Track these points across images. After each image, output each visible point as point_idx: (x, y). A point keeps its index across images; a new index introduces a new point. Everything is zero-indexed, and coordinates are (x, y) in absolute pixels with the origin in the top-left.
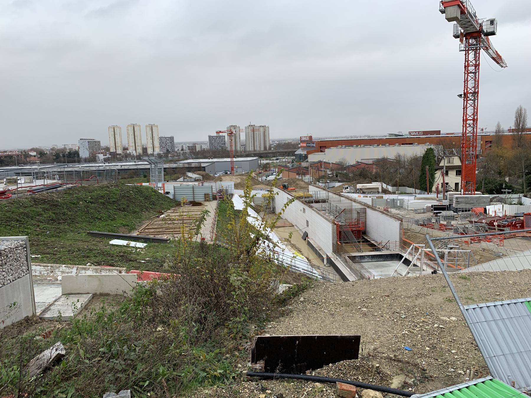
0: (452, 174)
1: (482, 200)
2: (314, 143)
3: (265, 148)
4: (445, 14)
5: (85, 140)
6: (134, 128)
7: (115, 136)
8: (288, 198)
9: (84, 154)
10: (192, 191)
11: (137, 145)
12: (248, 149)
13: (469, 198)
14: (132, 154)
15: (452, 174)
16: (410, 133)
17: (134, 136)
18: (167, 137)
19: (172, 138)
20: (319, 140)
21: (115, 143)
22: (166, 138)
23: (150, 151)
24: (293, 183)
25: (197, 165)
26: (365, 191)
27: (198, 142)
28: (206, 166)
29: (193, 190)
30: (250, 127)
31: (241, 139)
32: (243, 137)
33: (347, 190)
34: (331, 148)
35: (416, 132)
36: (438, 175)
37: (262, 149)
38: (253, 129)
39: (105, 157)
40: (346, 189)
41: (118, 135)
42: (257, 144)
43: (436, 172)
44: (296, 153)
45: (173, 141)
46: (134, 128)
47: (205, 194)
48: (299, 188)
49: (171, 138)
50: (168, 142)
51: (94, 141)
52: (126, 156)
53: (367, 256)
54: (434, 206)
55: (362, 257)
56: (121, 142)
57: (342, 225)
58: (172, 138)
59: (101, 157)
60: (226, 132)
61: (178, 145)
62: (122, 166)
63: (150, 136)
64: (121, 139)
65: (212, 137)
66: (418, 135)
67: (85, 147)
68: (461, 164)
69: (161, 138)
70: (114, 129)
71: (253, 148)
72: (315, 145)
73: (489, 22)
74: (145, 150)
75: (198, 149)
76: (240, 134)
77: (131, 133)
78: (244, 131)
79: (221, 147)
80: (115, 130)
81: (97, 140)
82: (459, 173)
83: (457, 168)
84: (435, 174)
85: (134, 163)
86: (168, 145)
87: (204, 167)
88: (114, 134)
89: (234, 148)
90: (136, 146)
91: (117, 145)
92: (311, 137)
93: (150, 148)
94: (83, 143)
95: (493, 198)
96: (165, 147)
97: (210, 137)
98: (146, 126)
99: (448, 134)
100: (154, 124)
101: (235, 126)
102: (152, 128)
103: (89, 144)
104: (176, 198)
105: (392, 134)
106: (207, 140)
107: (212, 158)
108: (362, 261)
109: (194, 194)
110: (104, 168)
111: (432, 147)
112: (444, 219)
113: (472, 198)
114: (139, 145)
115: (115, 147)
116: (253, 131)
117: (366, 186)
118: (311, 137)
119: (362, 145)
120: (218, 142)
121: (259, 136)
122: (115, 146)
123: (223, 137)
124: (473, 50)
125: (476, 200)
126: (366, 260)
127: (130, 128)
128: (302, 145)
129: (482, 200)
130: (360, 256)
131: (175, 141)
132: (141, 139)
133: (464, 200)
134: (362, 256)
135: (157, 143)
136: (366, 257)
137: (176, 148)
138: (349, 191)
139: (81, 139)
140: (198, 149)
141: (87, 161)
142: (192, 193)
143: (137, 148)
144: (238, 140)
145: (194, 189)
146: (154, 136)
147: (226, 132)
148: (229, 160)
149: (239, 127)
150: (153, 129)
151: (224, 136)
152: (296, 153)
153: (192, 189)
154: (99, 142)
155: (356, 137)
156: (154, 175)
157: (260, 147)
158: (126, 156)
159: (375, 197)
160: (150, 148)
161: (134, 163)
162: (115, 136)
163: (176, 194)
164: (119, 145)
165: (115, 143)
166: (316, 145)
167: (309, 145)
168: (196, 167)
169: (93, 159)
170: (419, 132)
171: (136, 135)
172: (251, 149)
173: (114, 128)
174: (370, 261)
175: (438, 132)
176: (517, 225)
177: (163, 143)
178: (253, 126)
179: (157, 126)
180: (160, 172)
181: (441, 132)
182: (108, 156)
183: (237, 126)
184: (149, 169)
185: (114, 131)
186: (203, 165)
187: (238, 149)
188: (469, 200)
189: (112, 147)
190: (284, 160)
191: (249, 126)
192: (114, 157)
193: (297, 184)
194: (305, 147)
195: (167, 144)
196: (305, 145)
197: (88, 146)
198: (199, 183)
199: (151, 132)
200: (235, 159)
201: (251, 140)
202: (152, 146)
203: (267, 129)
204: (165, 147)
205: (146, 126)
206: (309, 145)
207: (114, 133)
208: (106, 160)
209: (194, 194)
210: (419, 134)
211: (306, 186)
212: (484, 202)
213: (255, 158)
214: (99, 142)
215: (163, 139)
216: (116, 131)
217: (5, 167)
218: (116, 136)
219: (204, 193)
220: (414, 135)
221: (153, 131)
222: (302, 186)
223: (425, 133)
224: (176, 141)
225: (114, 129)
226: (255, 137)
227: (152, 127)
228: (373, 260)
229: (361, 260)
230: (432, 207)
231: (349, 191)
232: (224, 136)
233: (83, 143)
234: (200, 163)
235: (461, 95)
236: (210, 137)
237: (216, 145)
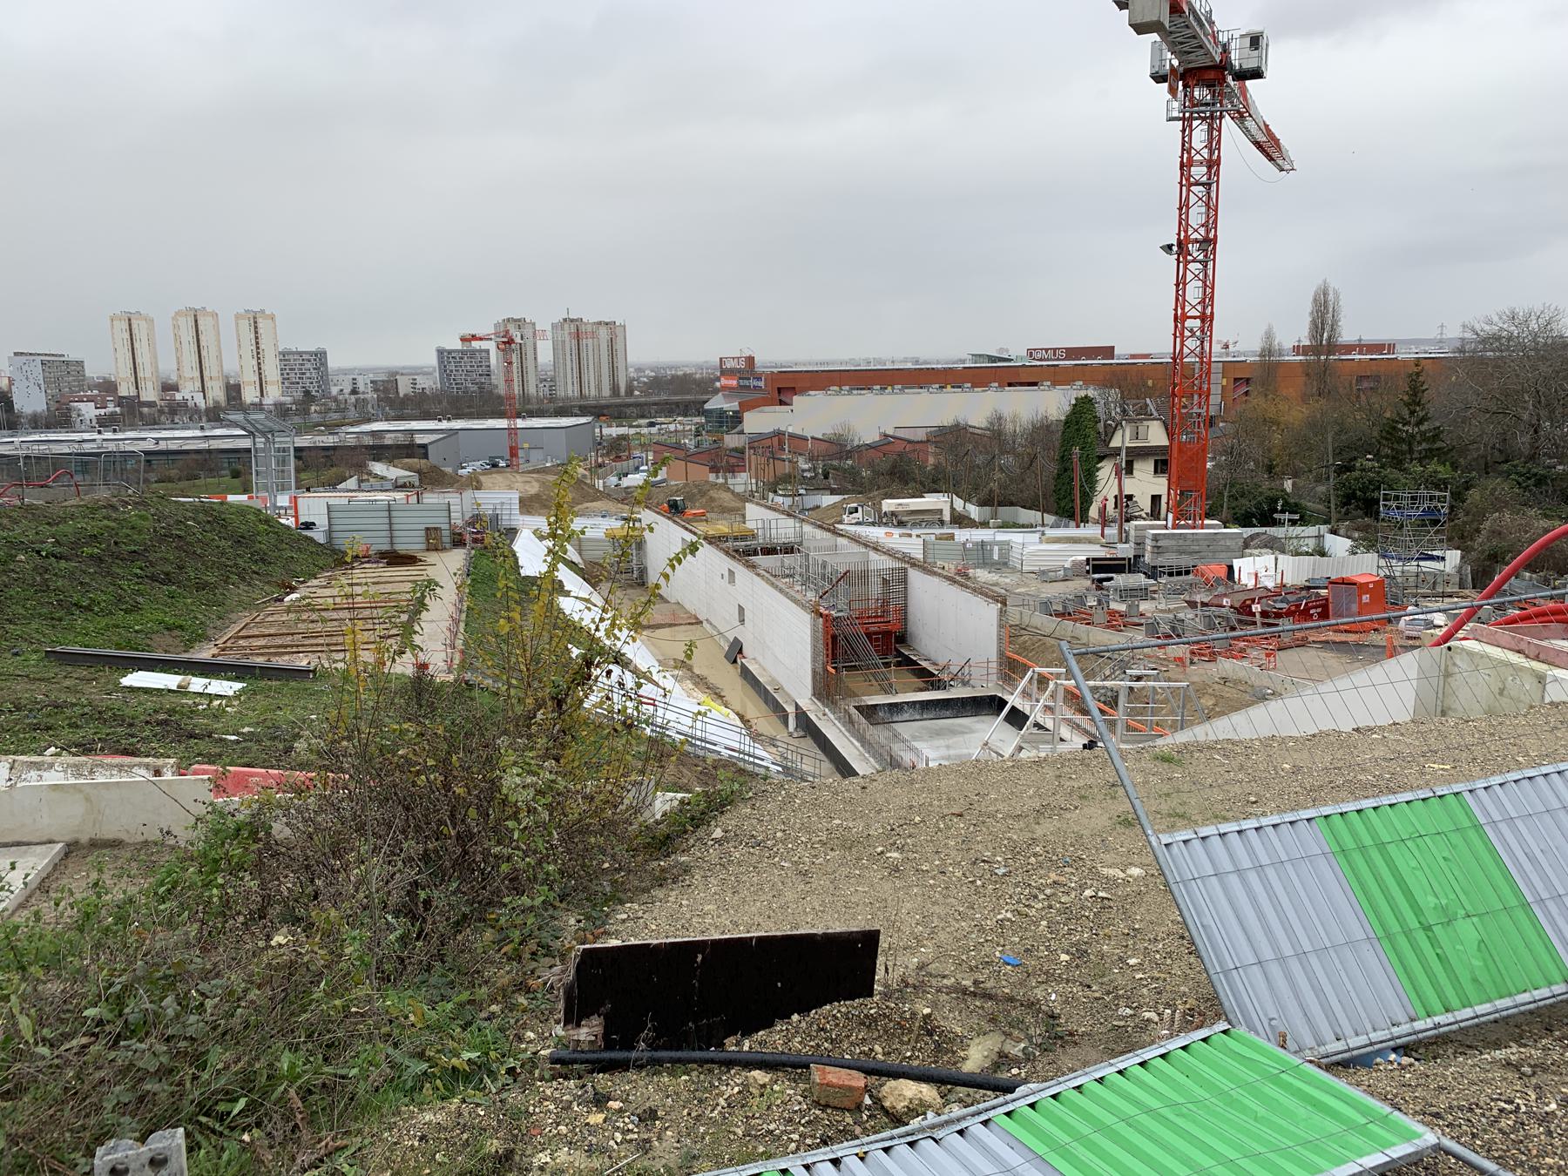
0: (1144, 469)
1: (1222, 543)
2: (759, 379)
3: (615, 389)
4: (1127, 11)
5: (32, 358)
6: (196, 321)
7: (132, 344)
8: (683, 539)
9: (30, 401)
10: (387, 521)
11: (206, 374)
12: (561, 393)
13: (1188, 537)
14: (190, 403)
15: (1144, 469)
16: (1030, 353)
17: (199, 346)
18: (306, 353)
19: (320, 356)
20: (775, 370)
21: (135, 368)
22: (301, 354)
23: (250, 395)
25: (401, 439)
26: (904, 519)
27: (404, 368)
28: (430, 443)
29: (390, 517)
30: (566, 326)
31: (540, 359)
32: (545, 353)
33: (854, 515)
34: (811, 392)
35: (1047, 350)
36: (1106, 471)
37: (606, 392)
38: (576, 331)
39: (102, 412)
40: (851, 513)
41: (145, 342)
42: (590, 377)
43: (1099, 465)
44: (707, 406)
45: (324, 364)
46: (196, 321)
47: (427, 529)
49: (316, 355)
50: (308, 365)
52: (174, 411)
53: (907, 703)
54: (1094, 559)
55: (895, 708)
56: (155, 364)
57: (840, 617)
58: (320, 356)
59: (89, 411)
60: (493, 337)
61: (341, 377)
62: (157, 440)
63: (248, 347)
64: (155, 357)
65: (450, 352)
66: (1051, 360)
67: (31, 380)
68: (1166, 443)
69: (284, 356)
70: (130, 325)
72: (762, 384)
73: (1248, 40)
74: (233, 391)
75: (404, 388)
76: (535, 344)
77: (188, 336)
78: (549, 334)
79: (477, 384)
80: (134, 326)
81: (73, 356)
82: (1161, 467)
83: (1157, 454)
84: (1098, 469)
85: (198, 433)
86: (308, 375)
87: (424, 446)
88: (132, 339)
89: (517, 390)
90: (206, 379)
91: (140, 374)
92: (750, 360)
93: (249, 384)
94: (25, 368)
95: (1252, 537)
96: (298, 383)
97: (441, 352)
98: (238, 317)
99: (1133, 356)
100: (263, 311)
101: (519, 320)
102: (255, 322)
103: (47, 369)
104: (336, 541)
105: (980, 355)
106: (432, 360)
107: (449, 419)
110: (99, 448)
111: (1091, 393)
112: (1121, 597)
113: (1195, 537)
114: (215, 374)
115: (133, 379)
116: (578, 335)
117: (908, 505)
118: (750, 360)
119: (896, 387)
120: (469, 368)
121: (594, 352)
122: (136, 378)
123: (484, 354)
124: (1204, 119)
125: (1207, 543)
126: (906, 716)
127: (182, 321)
128: (724, 381)
129: (1222, 543)
130: (891, 704)
131: (330, 364)
132: (219, 358)
133: (1173, 543)
134: (896, 705)
135: (272, 371)
137: (335, 385)
139: (16, 354)
140: (404, 388)
141: (37, 423)
143: (208, 384)
144: (530, 364)
145: (394, 514)
146: (262, 346)
147: (491, 339)
148: (502, 423)
149: (534, 324)
150: (260, 325)
151: (487, 351)
152: (707, 406)
154: (80, 363)
155: (880, 364)
156: (263, 470)
157: (599, 388)
158: (174, 411)
159: (933, 537)
160: (249, 384)
161: (198, 433)
162: (132, 344)
163: (335, 528)
164: (148, 375)
165: (135, 368)
166: (766, 386)
167: (746, 383)
168: (398, 447)
169: (60, 418)
170: (1055, 350)
171: (202, 344)
172: (570, 393)
173: (130, 320)
174: (918, 717)
175: (1108, 352)
176: (1311, 612)
177: (290, 369)
178: (576, 320)
179: (272, 318)
181: (1116, 352)
182: (111, 408)
183: (528, 320)
184: (248, 451)
185: (131, 330)
186: (420, 439)
187: (532, 390)
188: (1188, 543)
189: (123, 380)
190: (672, 427)
191: (565, 320)
192: (132, 412)
193: (712, 499)
194: (733, 388)
195: (304, 374)
196: (734, 383)
197: (41, 377)
198: (408, 496)
199: (253, 336)
200: (520, 423)
201: (570, 364)
203: (619, 331)
204: (298, 383)
205: (238, 317)
206: (746, 383)
207: (131, 335)
208: (104, 423)
210: (1055, 355)
212: (1228, 549)
213: (583, 420)
214: (80, 363)
215: (291, 357)
216: (135, 331)
218: (136, 345)
219: (423, 527)
220: (1041, 360)
221: (260, 331)
223: (1072, 353)
224: (333, 363)
225: (130, 325)
226: (583, 355)
227: (255, 318)
228: (925, 716)
229: (892, 715)
230: (1088, 564)
232: (487, 351)
233: (25, 368)
234: (412, 432)
235: (1170, 247)
236: (441, 352)
237: (461, 378)
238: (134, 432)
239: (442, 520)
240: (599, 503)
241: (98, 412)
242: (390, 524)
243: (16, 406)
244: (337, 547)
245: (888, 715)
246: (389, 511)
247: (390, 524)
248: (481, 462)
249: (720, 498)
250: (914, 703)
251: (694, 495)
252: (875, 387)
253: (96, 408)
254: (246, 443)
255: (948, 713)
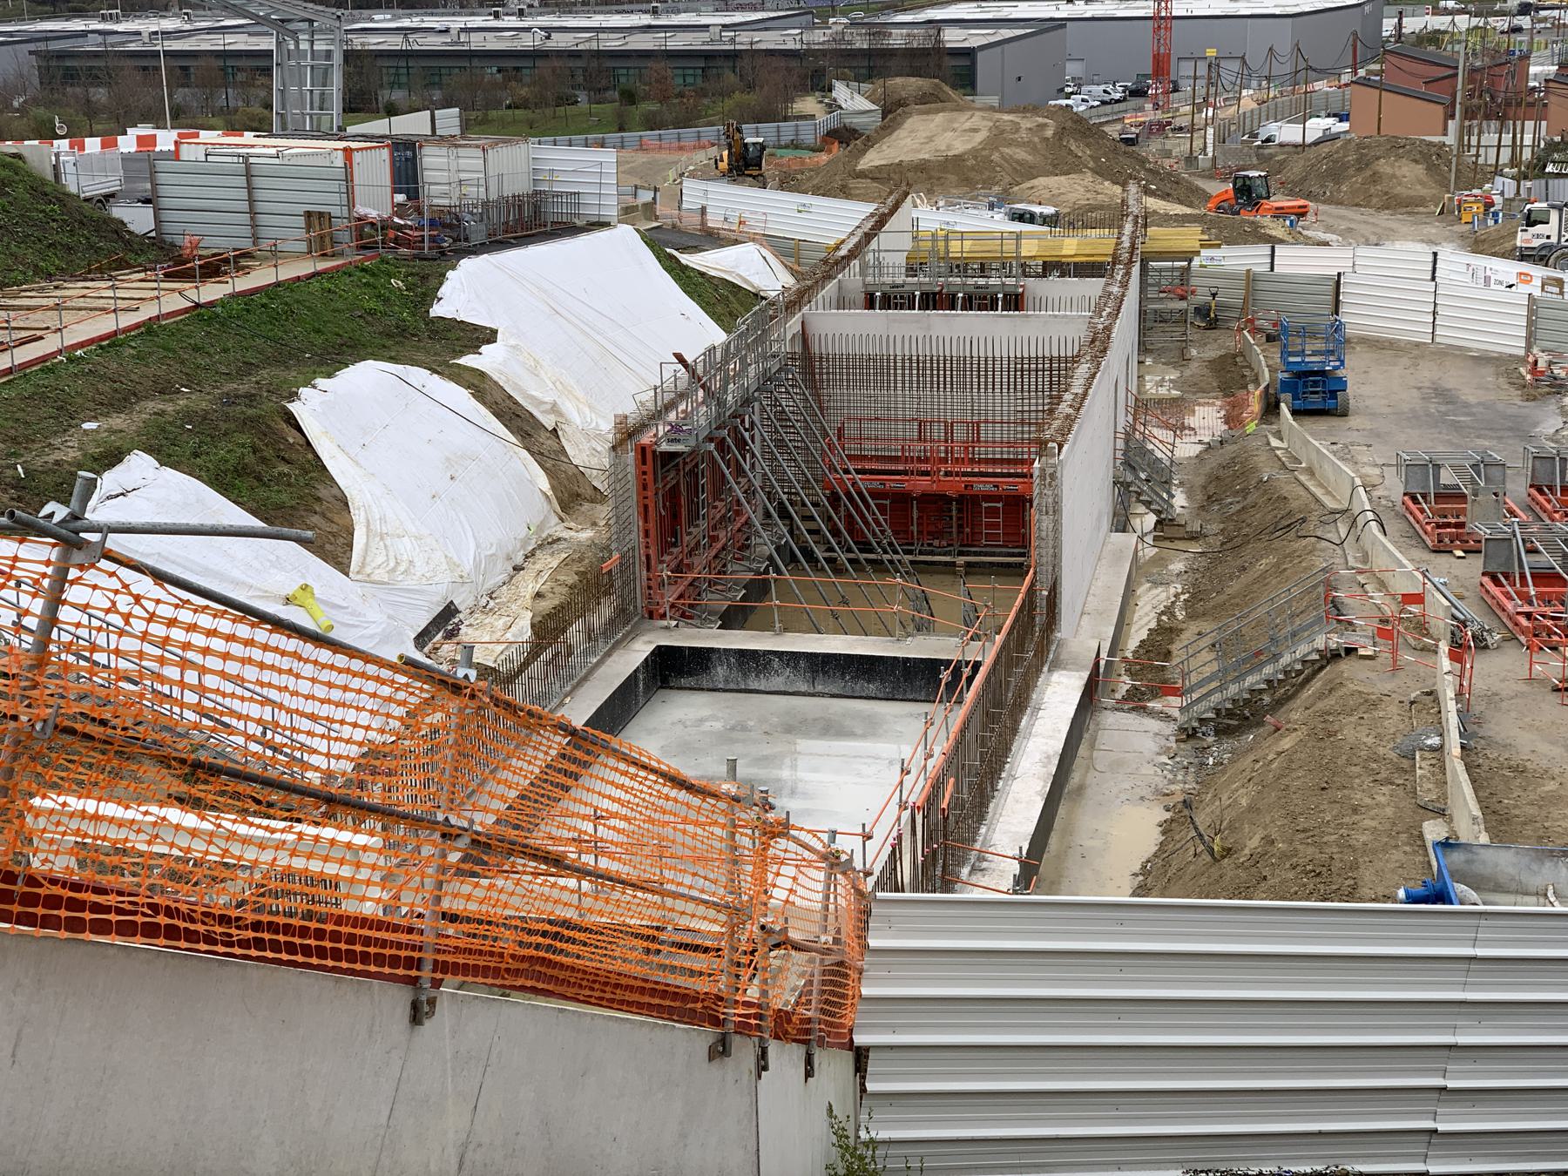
10: (244, 194)
24: (1351, 171)
29: (250, 188)
33: (1539, 228)
47: (308, 214)
48: (1375, 200)
62: (549, 31)
85: (646, 19)
87: (969, 53)
104: (167, 228)
108: (754, 685)
109: (253, 213)
110: (453, 43)
126: (777, 682)
130: (742, 654)
134: (754, 654)
136: (776, 663)
138: (1554, 240)
142: (245, 206)
145: (257, 182)
153: (242, 181)
161: (646, 19)
163: (260, 207)
168: (910, 53)
174: (804, 688)
180: (324, 77)
184: (268, 54)
186: (953, 38)
193: (1376, 178)
209: (253, 213)
211: (1423, 192)
217: (42, 19)
219: (302, 209)
222: (1398, 190)
228: (819, 688)
231: (1554, 240)
234: (938, 24)
238: (551, 18)
239: (335, 198)
240: (1063, 178)
242: (251, 201)
244: (168, 238)
245: (736, 674)
246: (249, 175)
247: (251, 201)
248: (1103, 87)
249: (1394, 176)
250: (792, 659)
251: (1345, 167)
254: (267, 43)
255: (872, 688)
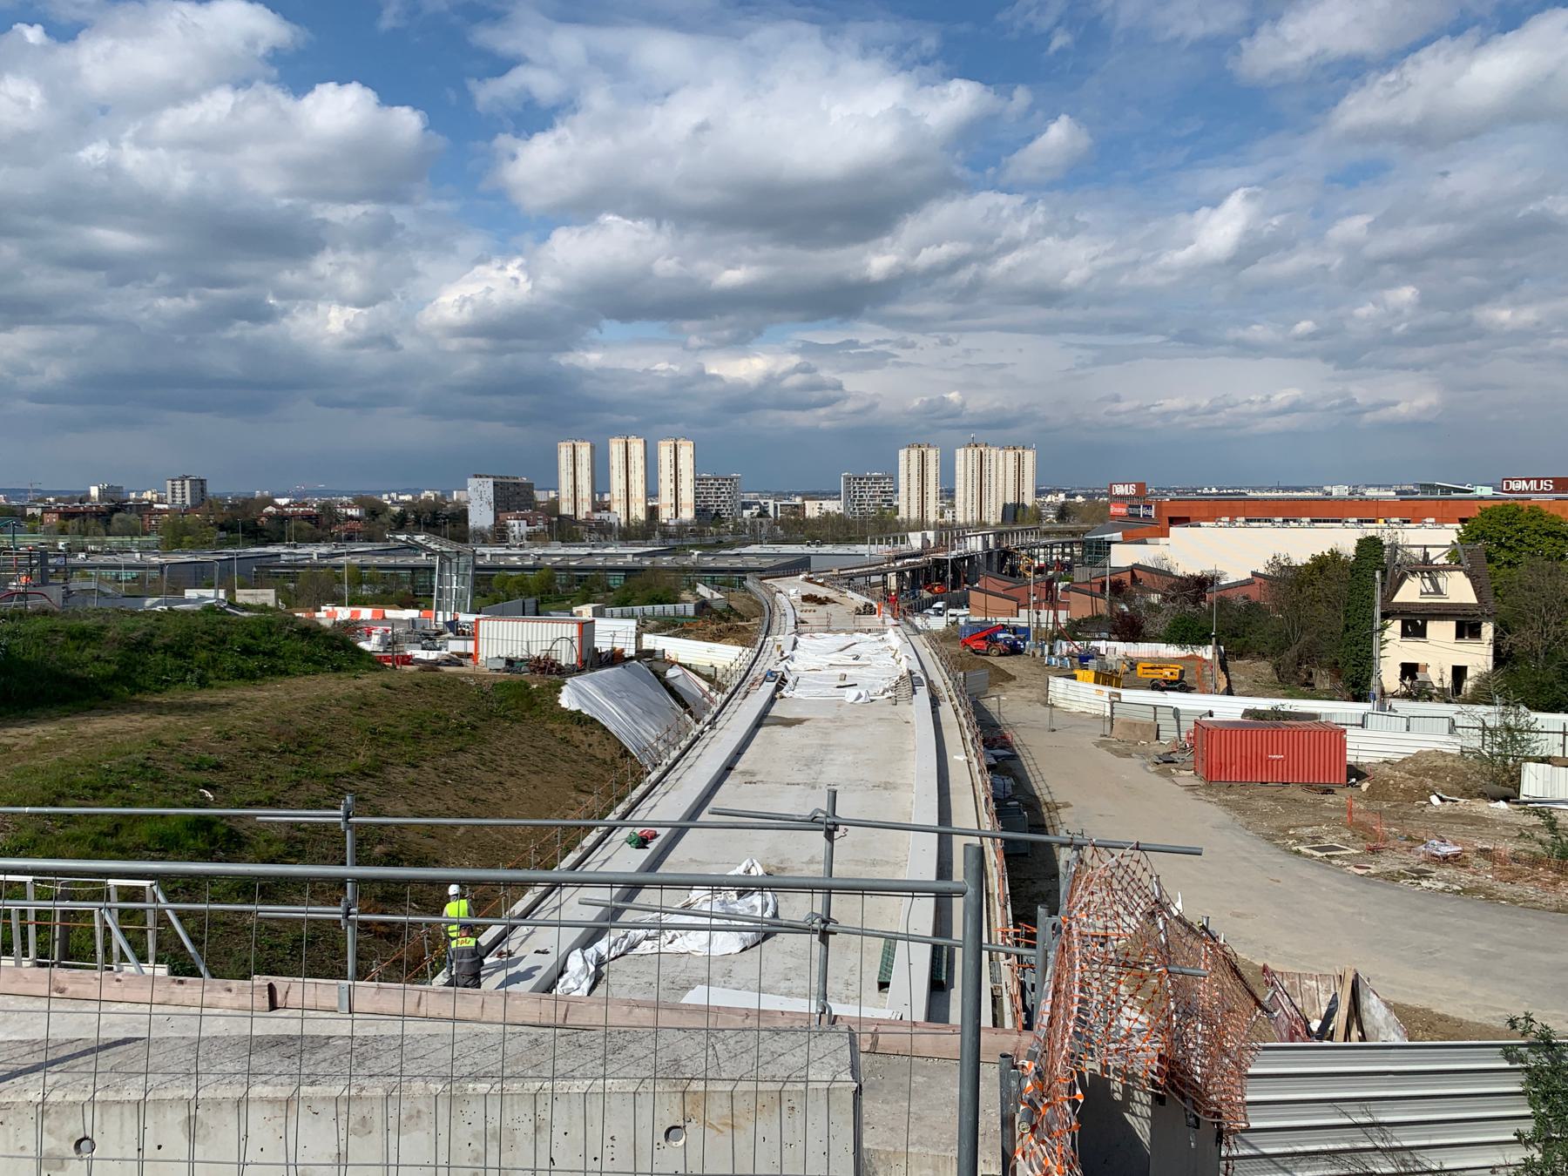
2: (1149, 507)
23: (666, 514)
51: (516, 481)
71: (976, 515)
93: (666, 506)
135: (687, 496)
141: (482, 537)
167: (1135, 511)
169: (499, 534)
182: (540, 526)
196: (1123, 511)
202: (673, 501)
210: (1538, 486)
218: (578, 469)
233: (480, 488)
241: (528, 529)
243: (470, 524)
252: (1277, 519)
253: (528, 525)
